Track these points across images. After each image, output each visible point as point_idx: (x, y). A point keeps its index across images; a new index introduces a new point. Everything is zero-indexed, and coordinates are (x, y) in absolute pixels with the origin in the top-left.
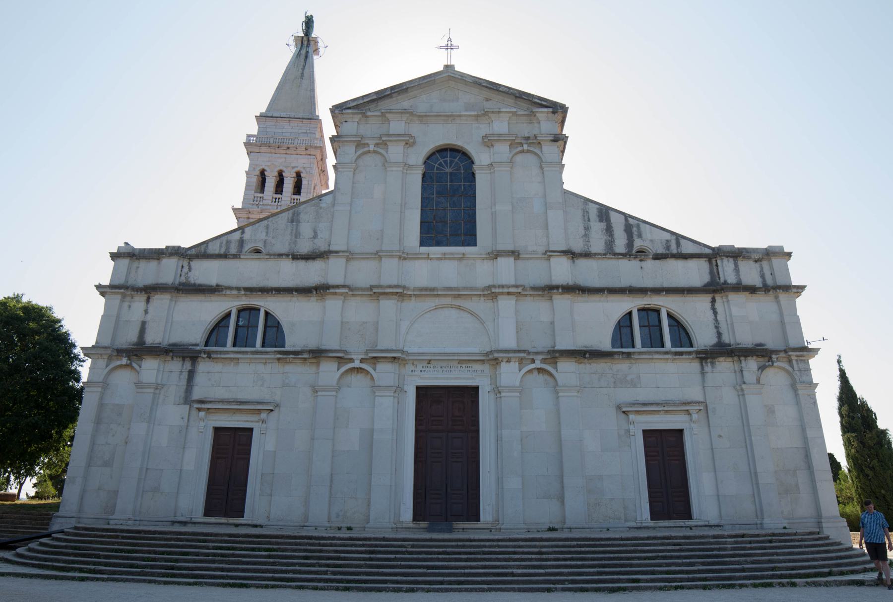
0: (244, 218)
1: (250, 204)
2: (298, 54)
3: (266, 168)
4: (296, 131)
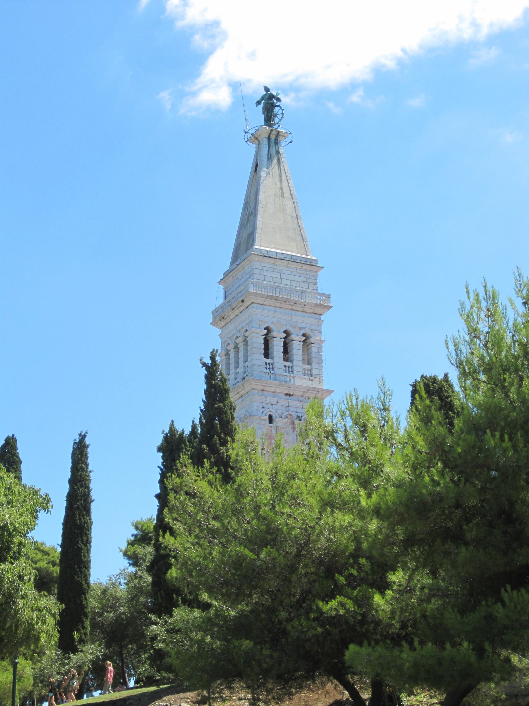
1: (262, 372)
2: (268, 155)
4: (295, 278)
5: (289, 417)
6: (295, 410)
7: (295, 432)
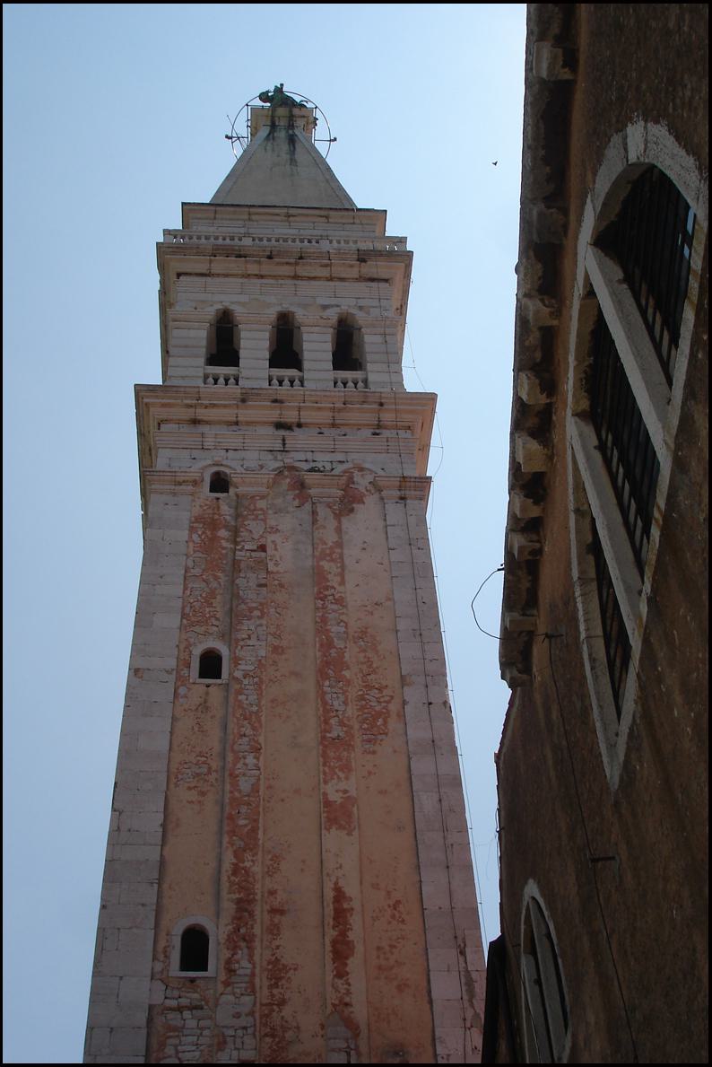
0: (179, 422)
3: (232, 307)
5: (286, 473)
6: (309, 456)
7: (308, 506)
